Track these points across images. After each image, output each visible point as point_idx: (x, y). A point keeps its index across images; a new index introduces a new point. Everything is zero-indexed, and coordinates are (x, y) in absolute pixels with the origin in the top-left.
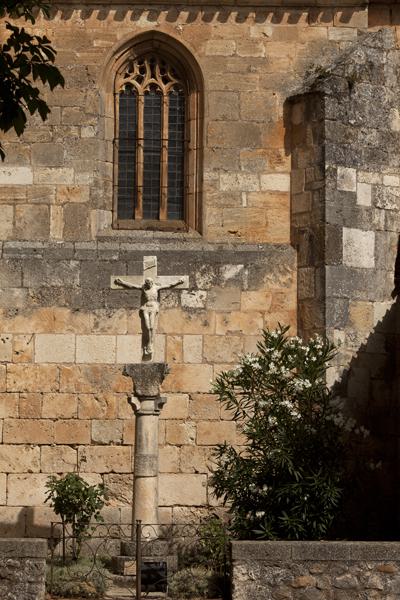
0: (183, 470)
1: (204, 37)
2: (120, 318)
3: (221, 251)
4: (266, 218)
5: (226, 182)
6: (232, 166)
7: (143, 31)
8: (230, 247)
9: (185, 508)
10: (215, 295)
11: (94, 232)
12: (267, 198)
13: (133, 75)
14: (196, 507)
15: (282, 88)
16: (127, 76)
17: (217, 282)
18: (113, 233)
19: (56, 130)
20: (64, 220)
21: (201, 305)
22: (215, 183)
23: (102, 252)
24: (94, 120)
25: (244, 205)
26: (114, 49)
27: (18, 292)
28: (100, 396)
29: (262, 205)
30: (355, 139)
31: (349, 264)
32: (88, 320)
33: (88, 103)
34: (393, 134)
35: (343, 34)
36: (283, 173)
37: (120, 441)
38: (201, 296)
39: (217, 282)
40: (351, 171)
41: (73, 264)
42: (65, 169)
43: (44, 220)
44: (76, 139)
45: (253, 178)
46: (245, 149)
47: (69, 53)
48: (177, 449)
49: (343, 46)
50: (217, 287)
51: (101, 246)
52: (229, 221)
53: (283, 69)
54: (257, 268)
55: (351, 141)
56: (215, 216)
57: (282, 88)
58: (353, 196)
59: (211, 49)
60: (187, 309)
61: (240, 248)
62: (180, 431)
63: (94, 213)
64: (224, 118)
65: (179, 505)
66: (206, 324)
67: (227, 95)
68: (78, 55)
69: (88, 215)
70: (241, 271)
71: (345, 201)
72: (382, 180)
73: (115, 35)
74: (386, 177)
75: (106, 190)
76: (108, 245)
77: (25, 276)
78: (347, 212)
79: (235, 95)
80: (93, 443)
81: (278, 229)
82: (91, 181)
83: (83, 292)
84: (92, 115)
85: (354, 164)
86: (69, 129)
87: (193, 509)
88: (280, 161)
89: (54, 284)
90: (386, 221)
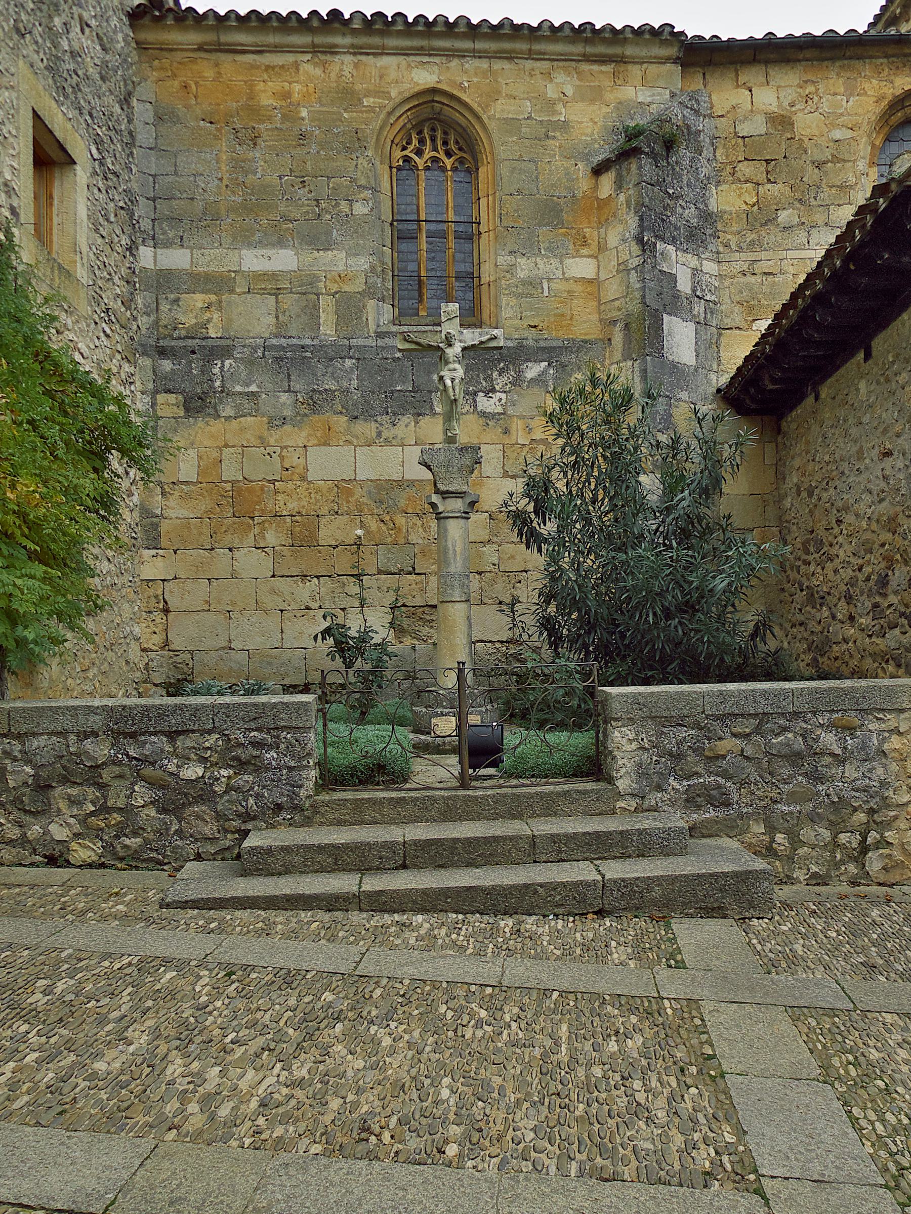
0: (486, 600)
1: (494, 95)
2: (406, 426)
3: (521, 347)
4: (571, 309)
5: (524, 267)
6: (529, 248)
7: (422, 87)
8: (531, 342)
9: (489, 644)
10: (516, 397)
11: (372, 327)
12: (572, 286)
13: (411, 147)
14: (502, 642)
15: (586, 157)
16: (404, 148)
17: (517, 382)
18: (394, 329)
19: (323, 205)
20: (336, 313)
21: (499, 409)
22: (511, 269)
23: (383, 348)
24: (367, 194)
25: (546, 294)
26: (388, 109)
27: (284, 397)
28: (387, 518)
29: (565, 295)
30: (673, 212)
31: (671, 359)
32: (367, 428)
33: (359, 173)
34: (710, 215)
35: (654, 95)
36: (589, 256)
37: (411, 569)
38: (500, 400)
39: (517, 382)
40: (671, 248)
41: (349, 363)
42: (335, 252)
43: (313, 311)
44: (347, 216)
45: (555, 262)
46: (544, 228)
47: (334, 113)
48: (477, 576)
49: (654, 108)
50: (517, 388)
51: (380, 342)
52: (528, 313)
53: (587, 135)
54: (563, 366)
55: (669, 214)
56: (512, 307)
57: (586, 157)
58: (673, 278)
59: (503, 111)
60: (483, 414)
61: (542, 344)
62: (480, 556)
63: (371, 304)
64: (519, 192)
65: (482, 641)
66: (506, 432)
67: (523, 165)
68: (345, 115)
69: (364, 306)
70: (544, 373)
71: (665, 284)
72: (701, 265)
73: (388, 93)
74: (704, 262)
75: (384, 279)
76: (388, 341)
77: (292, 378)
78: (667, 299)
79: (531, 166)
80: (380, 572)
81: (585, 322)
82: (366, 266)
83: (362, 396)
84: (365, 188)
85: (673, 242)
86: (337, 205)
87: (498, 645)
88: (585, 243)
89: (327, 387)
90: (706, 313)
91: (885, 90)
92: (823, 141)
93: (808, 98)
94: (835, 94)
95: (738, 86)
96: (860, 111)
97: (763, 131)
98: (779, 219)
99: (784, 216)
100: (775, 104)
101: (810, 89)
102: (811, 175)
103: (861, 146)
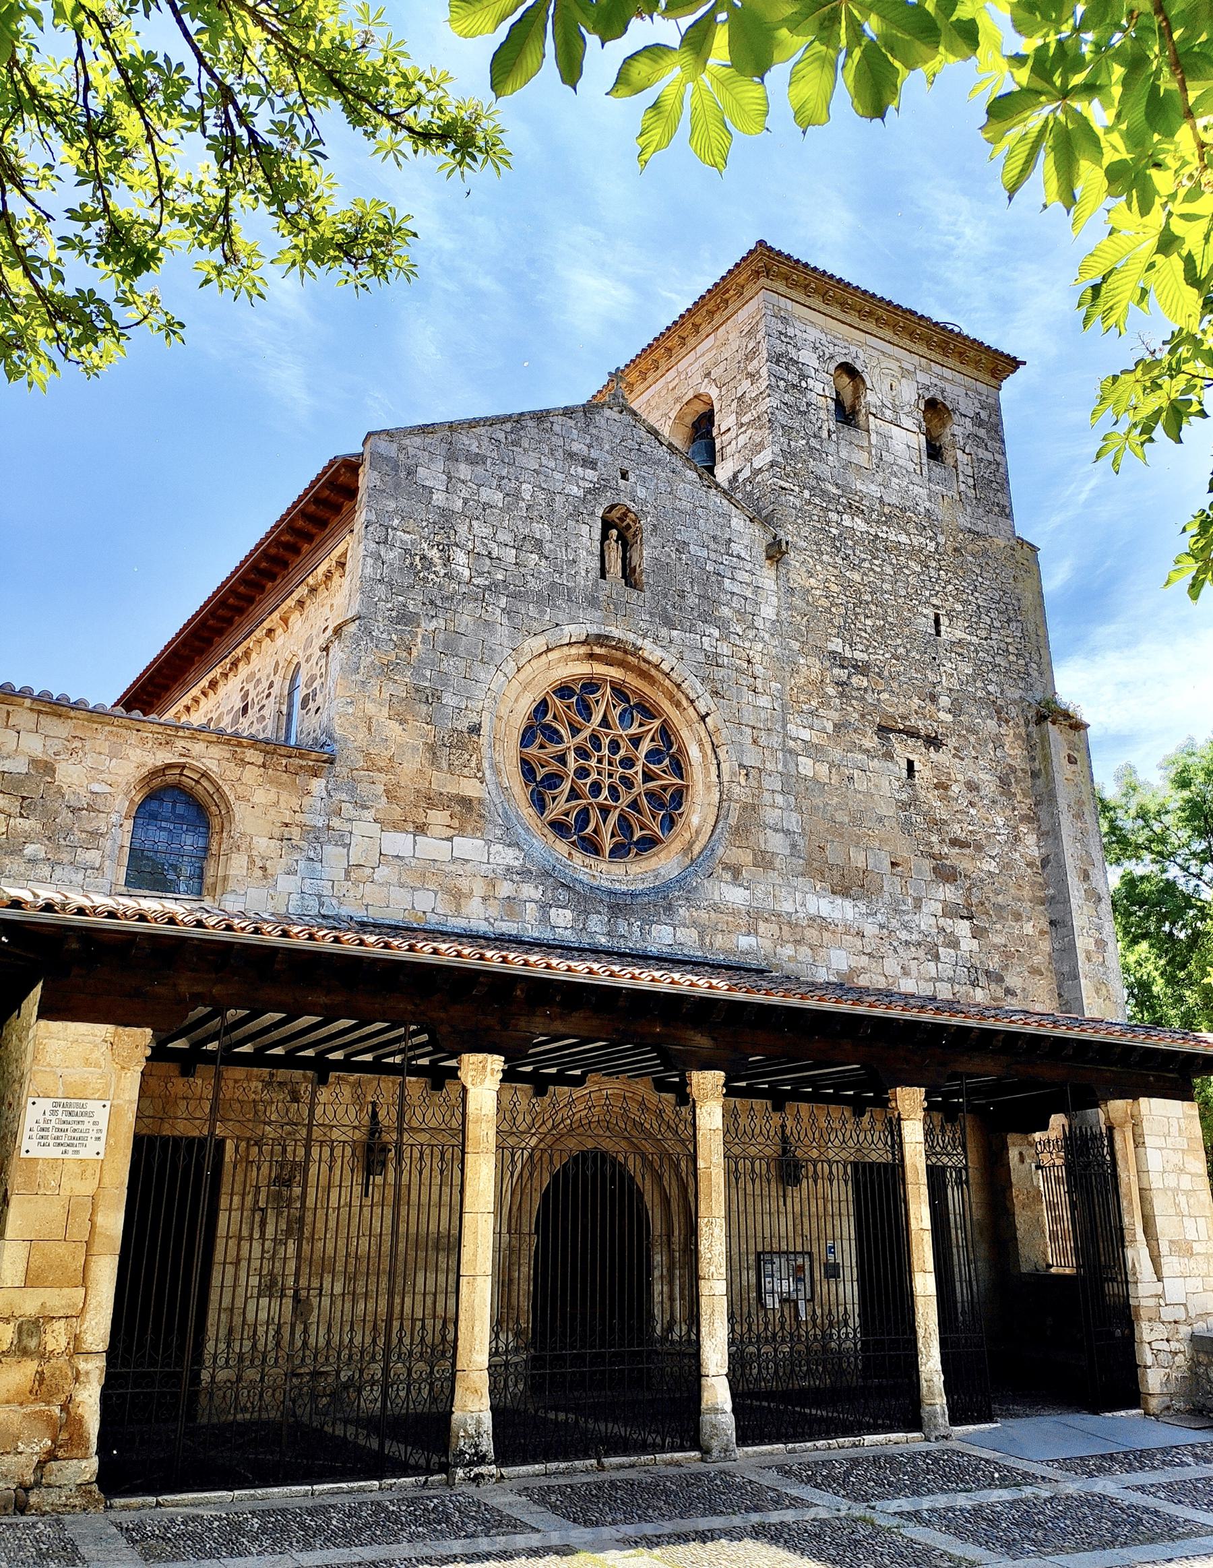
91: (147, 759)
92: (82, 792)
93: (73, 752)
94: (100, 753)
95: (7, 727)
96: (121, 772)
97: (25, 770)
98: (25, 852)
99: (29, 850)
100: (41, 749)
101: (77, 744)
102: (65, 817)
103: (117, 802)
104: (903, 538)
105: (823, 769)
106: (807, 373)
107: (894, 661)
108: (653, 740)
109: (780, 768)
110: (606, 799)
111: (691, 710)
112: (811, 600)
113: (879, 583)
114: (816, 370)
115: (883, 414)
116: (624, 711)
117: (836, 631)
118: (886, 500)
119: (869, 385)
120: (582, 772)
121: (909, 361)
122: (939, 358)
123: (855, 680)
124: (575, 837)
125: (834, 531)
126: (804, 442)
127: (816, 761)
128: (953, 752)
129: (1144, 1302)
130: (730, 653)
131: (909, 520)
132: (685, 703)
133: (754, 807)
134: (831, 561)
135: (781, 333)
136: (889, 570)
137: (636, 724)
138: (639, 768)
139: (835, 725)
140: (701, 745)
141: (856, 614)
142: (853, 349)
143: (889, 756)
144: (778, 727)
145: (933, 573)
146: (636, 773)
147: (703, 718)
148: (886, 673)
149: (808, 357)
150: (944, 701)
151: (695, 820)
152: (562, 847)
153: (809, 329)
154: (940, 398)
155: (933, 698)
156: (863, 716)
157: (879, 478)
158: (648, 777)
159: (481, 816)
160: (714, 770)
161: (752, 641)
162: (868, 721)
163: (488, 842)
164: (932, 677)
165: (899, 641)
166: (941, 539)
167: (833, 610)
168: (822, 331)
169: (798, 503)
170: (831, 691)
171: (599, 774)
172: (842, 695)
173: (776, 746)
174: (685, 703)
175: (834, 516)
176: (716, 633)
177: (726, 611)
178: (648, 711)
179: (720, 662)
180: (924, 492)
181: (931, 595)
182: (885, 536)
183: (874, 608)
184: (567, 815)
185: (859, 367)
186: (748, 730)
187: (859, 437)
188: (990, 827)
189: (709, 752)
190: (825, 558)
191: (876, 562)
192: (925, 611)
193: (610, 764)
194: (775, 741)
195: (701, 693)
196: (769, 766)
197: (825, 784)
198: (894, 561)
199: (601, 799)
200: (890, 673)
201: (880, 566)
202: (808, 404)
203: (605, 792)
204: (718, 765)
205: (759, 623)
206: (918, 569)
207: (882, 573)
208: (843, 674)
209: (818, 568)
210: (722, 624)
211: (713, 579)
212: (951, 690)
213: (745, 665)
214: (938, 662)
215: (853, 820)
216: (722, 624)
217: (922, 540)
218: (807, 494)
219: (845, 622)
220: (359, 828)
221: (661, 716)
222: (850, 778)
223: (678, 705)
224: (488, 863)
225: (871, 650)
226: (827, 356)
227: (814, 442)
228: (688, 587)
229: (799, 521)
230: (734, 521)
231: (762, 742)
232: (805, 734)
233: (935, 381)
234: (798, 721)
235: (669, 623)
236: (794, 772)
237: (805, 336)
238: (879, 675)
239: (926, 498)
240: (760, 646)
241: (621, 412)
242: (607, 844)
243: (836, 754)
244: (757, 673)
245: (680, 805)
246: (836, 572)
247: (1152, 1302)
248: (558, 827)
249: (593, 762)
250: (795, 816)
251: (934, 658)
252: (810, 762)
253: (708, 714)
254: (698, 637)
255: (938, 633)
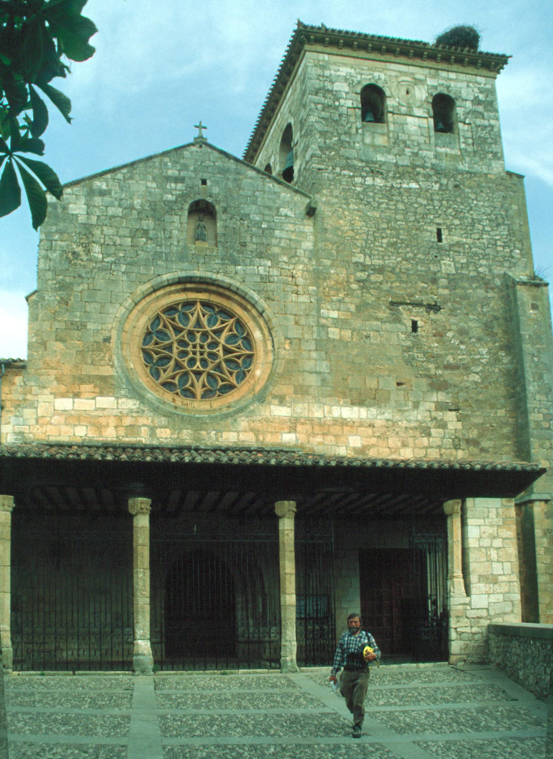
104: (414, 185)
105: (347, 334)
106: (339, 96)
107: (404, 262)
108: (231, 330)
109: (315, 336)
110: (198, 367)
111: (254, 312)
112: (340, 233)
113: (393, 216)
114: (347, 93)
115: (399, 110)
116: (211, 316)
117: (359, 250)
118: (400, 163)
119: (388, 93)
120: (184, 354)
121: (420, 73)
122: (444, 66)
123: (373, 278)
124: (179, 391)
125: (359, 189)
126: (336, 139)
127: (341, 329)
128: (449, 312)
129: (453, 608)
130: (279, 274)
131: (418, 174)
132: (249, 307)
133: (295, 361)
134: (356, 207)
135: (320, 75)
136: (401, 206)
137: (219, 322)
138: (220, 348)
139: (358, 308)
140: (261, 329)
141: (375, 238)
142: (376, 74)
143: (398, 320)
144: (314, 313)
145: (436, 203)
146: (218, 351)
147: (261, 314)
148: (397, 270)
149: (341, 87)
150: (443, 282)
151: (258, 373)
152: (168, 396)
153: (341, 69)
154: (446, 92)
155: (434, 281)
156: (378, 298)
157: (395, 151)
158: (227, 351)
159: (112, 385)
160: (269, 343)
161: (294, 264)
162: (382, 301)
163: (117, 398)
164: (433, 268)
165: (408, 250)
166: (444, 181)
167: (357, 237)
168: (352, 68)
169: (331, 176)
170: (354, 286)
171: (194, 353)
172: (362, 288)
173: (312, 324)
174: (249, 307)
175: (358, 180)
176: (269, 263)
177: (276, 250)
178: (229, 314)
179: (272, 280)
180: (431, 154)
181: (435, 218)
182: (399, 186)
183: (388, 232)
184: (173, 378)
185: (380, 84)
186: (292, 317)
187: (379, 128)
188: (475, 355)
189: (267, 333)
190: (351, 207)
191: (392, 203)
192: (429, 228)
193: (202, 347)
194: (312, 321)
195: (257, 299)
196: (306, 336)
197: (348, 342)
198: (406, 201)
199: (195, 368)
200: (400, 269)
201: (395, 205)
202: (340, 115)
203: (198, 364)
204: (273, 340)
205: (300, 252)
206: (425, 202)
207: (396, 209)
208: (362, 275)
209: (346, 213)
210: (273, 258)
211: (267, 232)
212: (448, 274)
213: (290, 279)
214: (439, 258)
215: (369, 361)
216: (273, 258)
217: (429, 183)
218: (338, 170)
219: (366, 243)
220: (41, 398)
221: (235, 316)
222: (367, 337)
223: (246, 309)
224: (118, 408)
225: (386, 258)
226: (355, 82)
227: (343, 137)
228: (248, 239)
229: (332, 187)
230: (283, 195)
231: (303, 321)
232: (334, 314)
233: (441, 82)
234: (329, 307)
235: (235, 263)
236: (325, 338)
237: (338, 73)
238: (392, 272)
239: (432, 157)
240: (301, 267)
241: (201, 146)
242: (199, 391)
243: (357, 324)
244: (298, 283)
245: (250, 365)
246: (359, 213)
247: (460, 607)
248: (168, 385)
249: (190, 349)
250: (325, 364)
251: (436, 257)
252: (337, 330)
253: (263, 312)
254: (256, 267)
255: (440, 239)
